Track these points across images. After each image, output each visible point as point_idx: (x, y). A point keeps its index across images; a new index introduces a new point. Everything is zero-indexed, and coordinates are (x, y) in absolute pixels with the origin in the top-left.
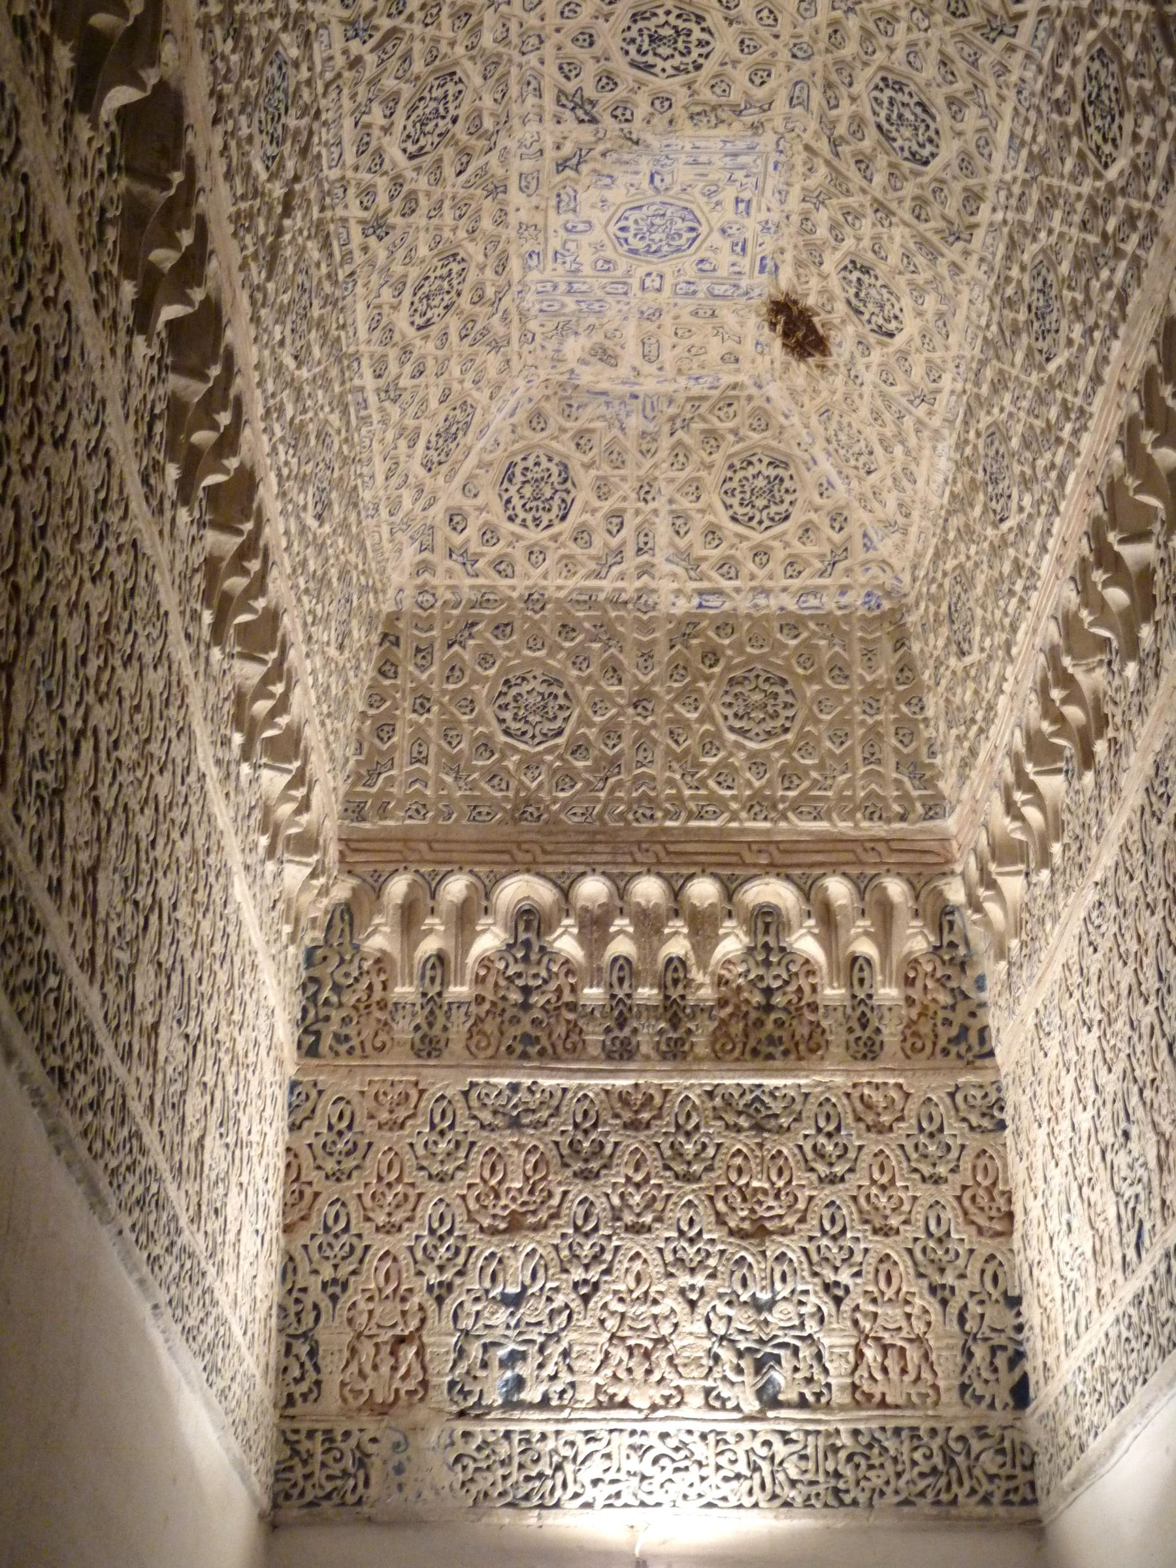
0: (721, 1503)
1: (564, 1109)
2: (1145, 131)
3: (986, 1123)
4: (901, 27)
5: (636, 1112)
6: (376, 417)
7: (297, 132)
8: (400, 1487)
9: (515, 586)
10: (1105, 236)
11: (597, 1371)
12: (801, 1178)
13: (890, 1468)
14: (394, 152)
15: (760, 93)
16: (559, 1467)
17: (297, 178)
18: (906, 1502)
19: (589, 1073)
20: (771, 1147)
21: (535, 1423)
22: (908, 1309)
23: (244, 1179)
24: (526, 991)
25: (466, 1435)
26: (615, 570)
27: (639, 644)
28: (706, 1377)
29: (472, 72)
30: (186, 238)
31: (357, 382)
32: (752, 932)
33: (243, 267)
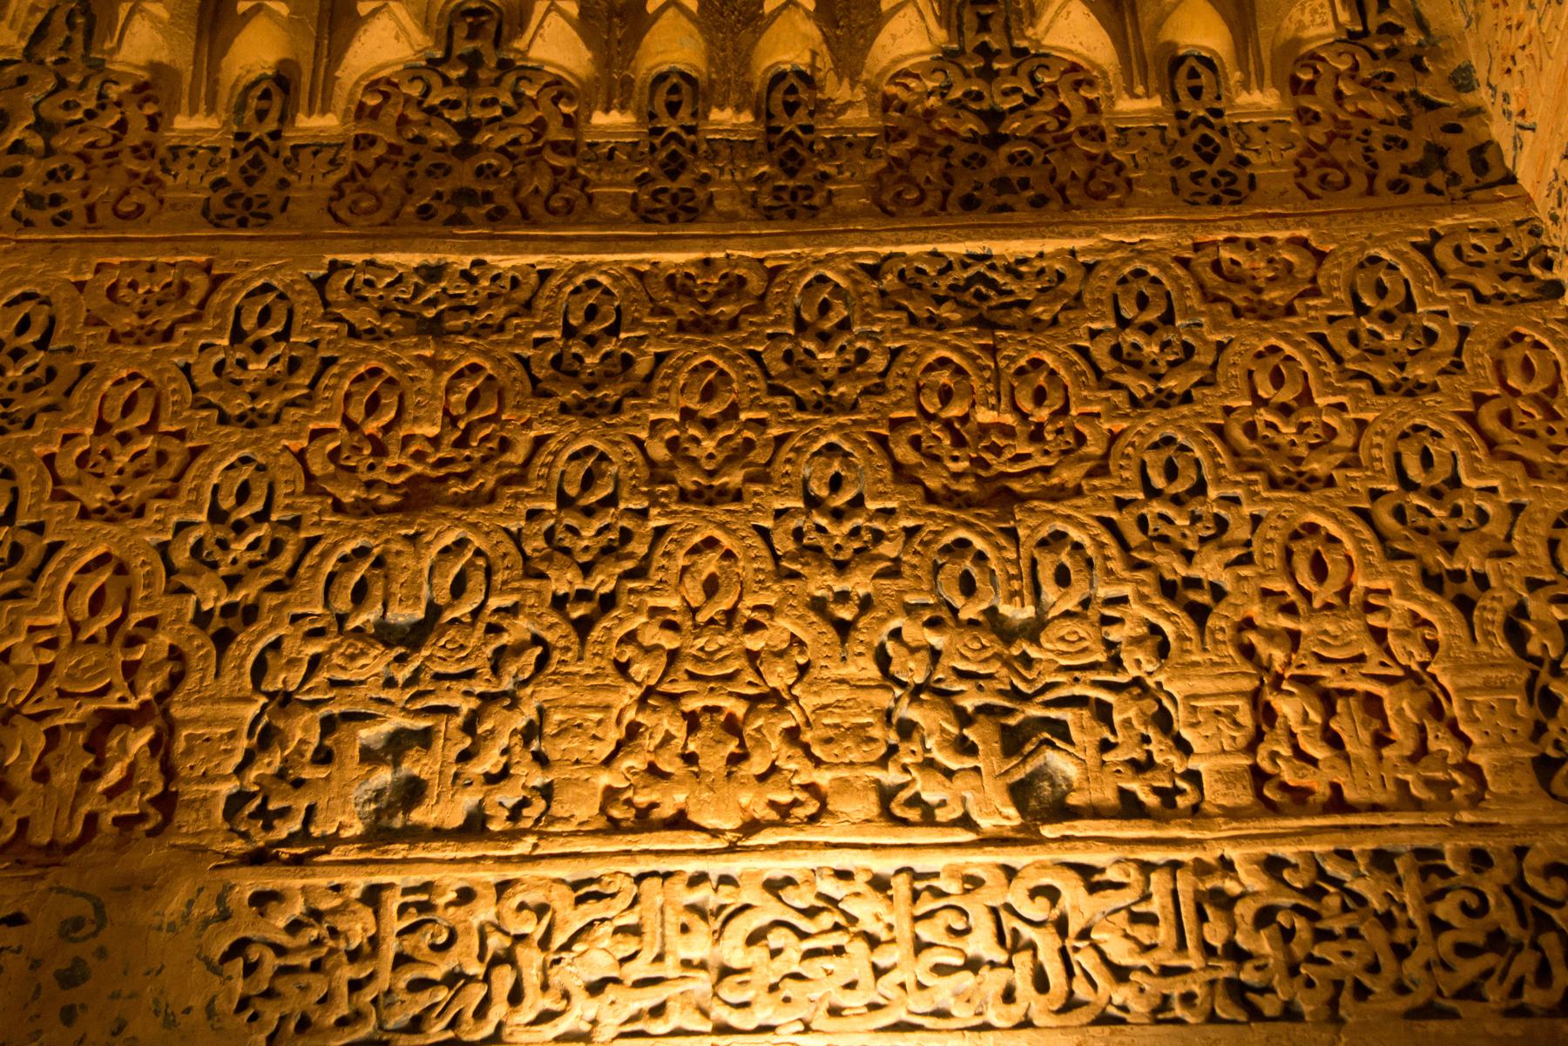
0: (928, 1022)
1: (542, 304)
3: (1514, 288)
8: (68, 1015)
11: (608, 762)
13: (1375, 936)
19: (601, 244)
22: (1376, 620)
25: (263, 900)
28: (883, 763)
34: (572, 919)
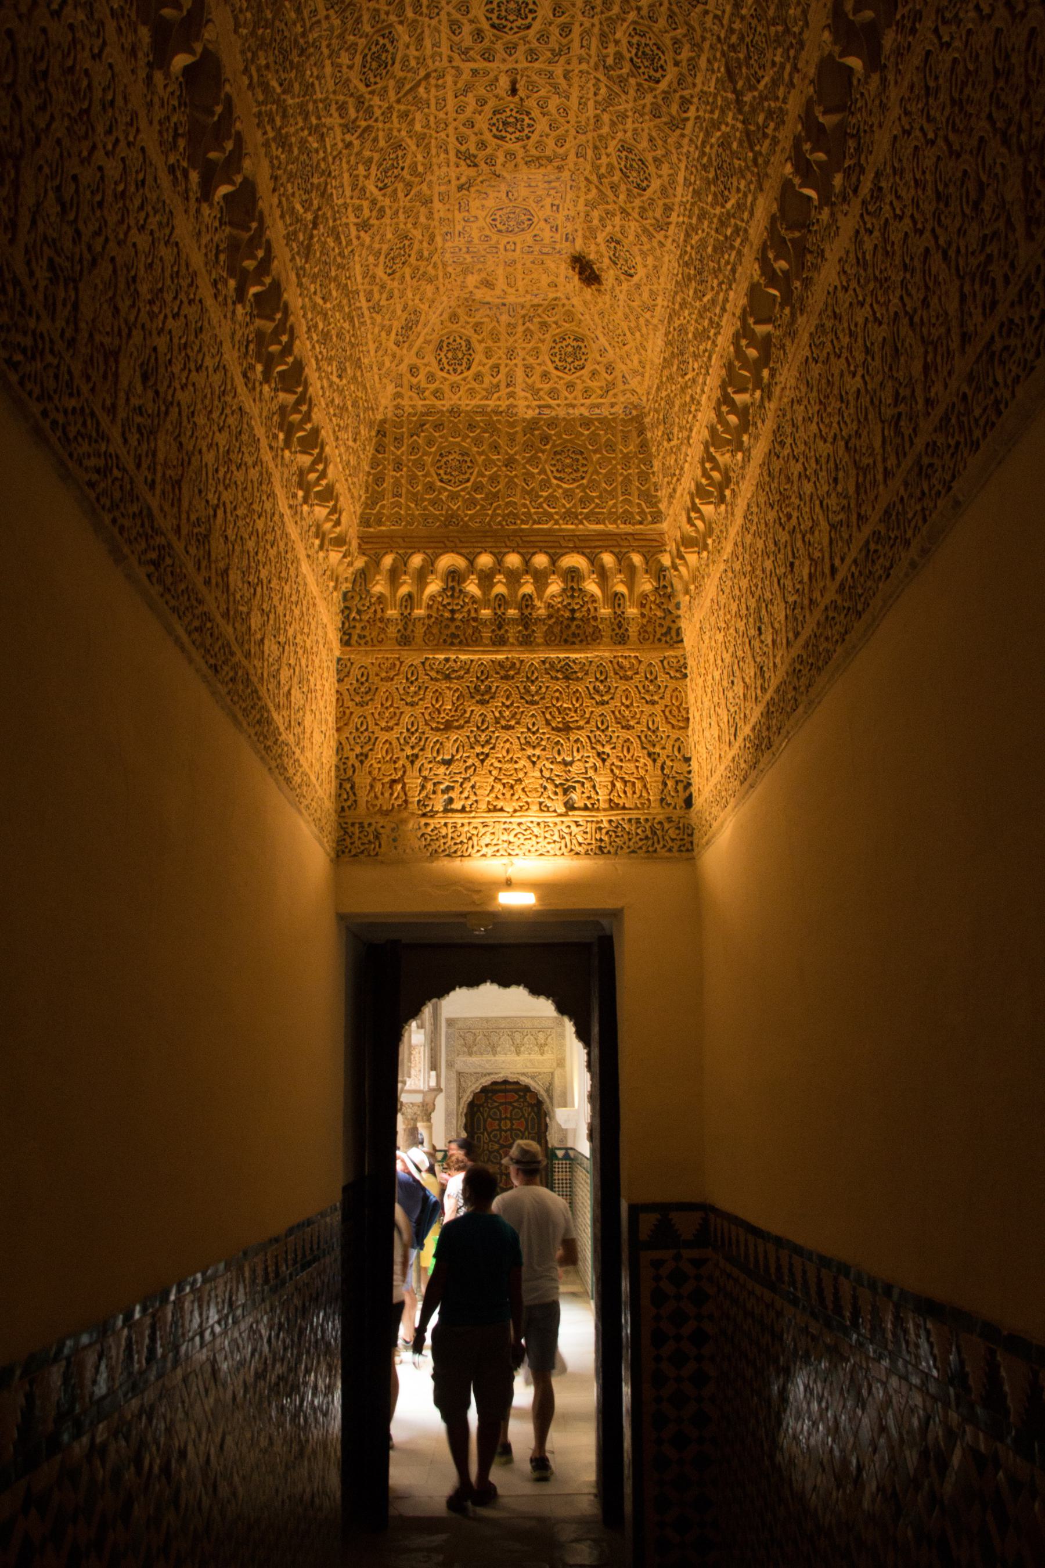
2: (742, 187)
3: (678, 675)
4: (629, 120)
5: (506, 671)
6: (368, 322)
7: (319, 184)
9: (444, 405)
10: (726, 237)
12: (587, 702)
13: (626, 837)
14: (371, 187)
15: (561, 151)
16: (470, 838)
17: (319, 209)
18: (633, 852)
19: (484, 652)
20: (573, 688)
21: (458, 819)
23: (314, 707)
24: (453, 611)
26: (496, 396)
27: (508, 434)
29: (411, 144)
30: (260, 254)
31: (358, 304)
32: (565, 581)
33: (293, 259)
34: (482, 830)
